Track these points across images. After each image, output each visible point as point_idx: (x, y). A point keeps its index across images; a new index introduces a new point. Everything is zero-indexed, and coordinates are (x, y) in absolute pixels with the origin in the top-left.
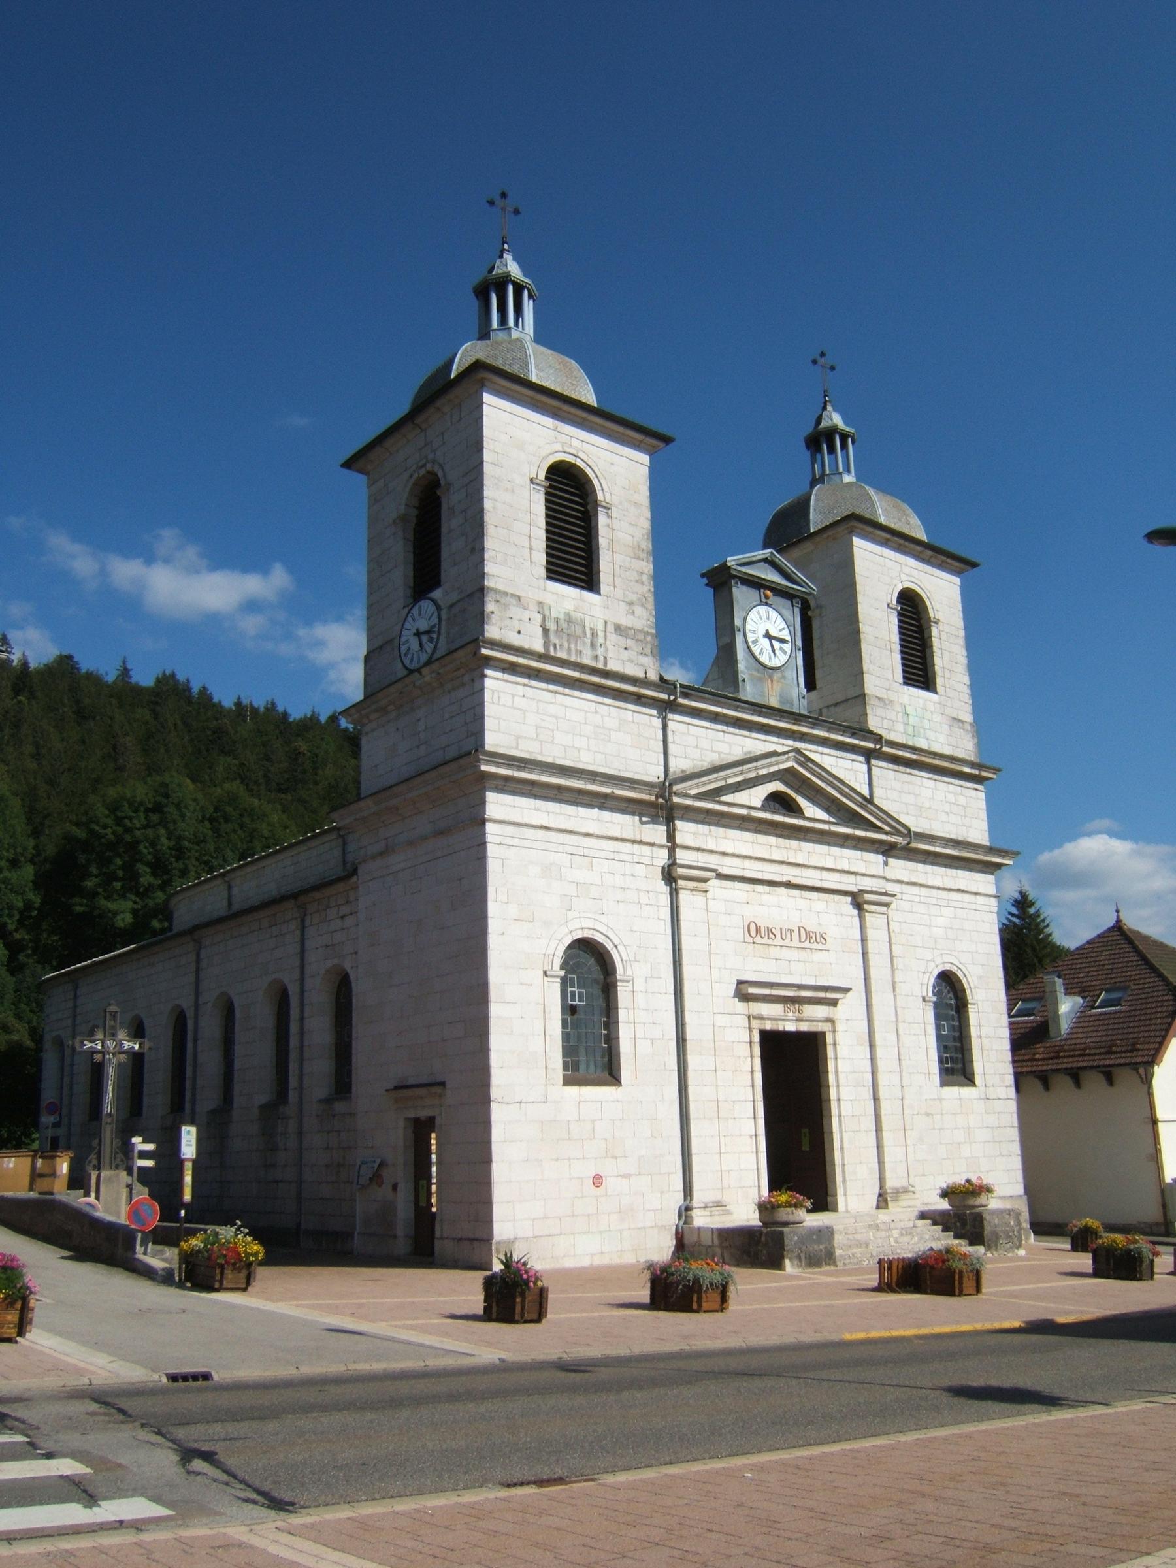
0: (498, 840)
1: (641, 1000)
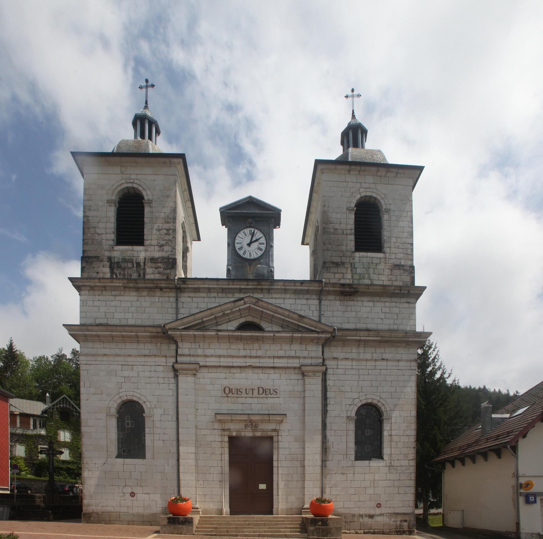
1: (158, 424)
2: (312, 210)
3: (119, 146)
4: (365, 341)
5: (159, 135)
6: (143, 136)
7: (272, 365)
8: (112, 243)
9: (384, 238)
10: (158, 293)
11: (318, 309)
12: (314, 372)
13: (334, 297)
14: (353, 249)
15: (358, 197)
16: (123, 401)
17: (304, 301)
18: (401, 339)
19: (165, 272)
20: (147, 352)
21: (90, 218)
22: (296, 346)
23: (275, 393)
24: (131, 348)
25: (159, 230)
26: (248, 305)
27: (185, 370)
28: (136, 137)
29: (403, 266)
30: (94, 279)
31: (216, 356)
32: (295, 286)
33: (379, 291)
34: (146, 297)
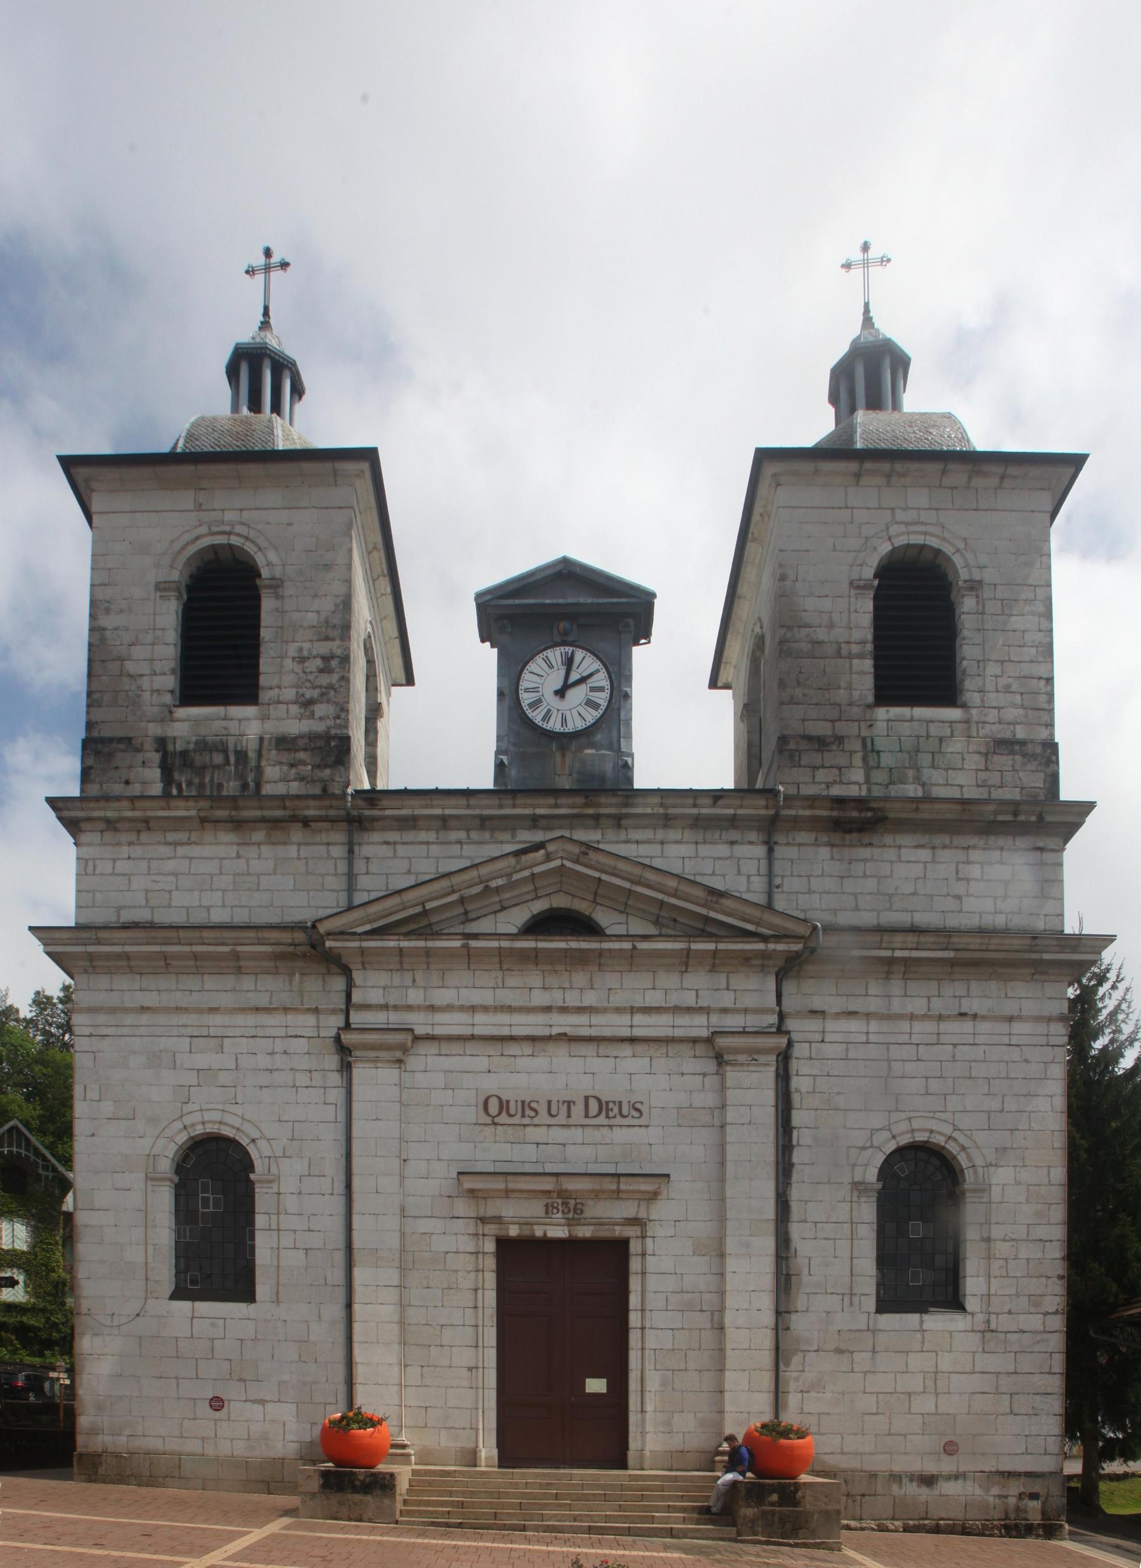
0: (87, 1031)
2: (743, 589)
3: (190, 436)
4: (906, 961)
5: (300, 398)
6: (255, 405)
7: (625, 1032)
8: (168, 699)
9: (965, 663)
10: (297, 834)
11: (764, 870)
12: (752, 1051)
13: (813, 835)
14: (870, 699)
15: (885, 548)
16: (192, 1138)
17: (723, 850)
18: (1017, 956)
19: (319, 774)
20: (263, 1000)
21: (108, 634)
22: (698, 979)
23: (636, 1114)
24: (218, 989)
25: (302, 660)
26: (558, 863)
27: (373, 1047)
28: (235, 408)
29: (1022, 743)
30: (118, 799)
31: (462, 1008)
32: (695, 806)
33: (948, 816)
34: (263, 848)
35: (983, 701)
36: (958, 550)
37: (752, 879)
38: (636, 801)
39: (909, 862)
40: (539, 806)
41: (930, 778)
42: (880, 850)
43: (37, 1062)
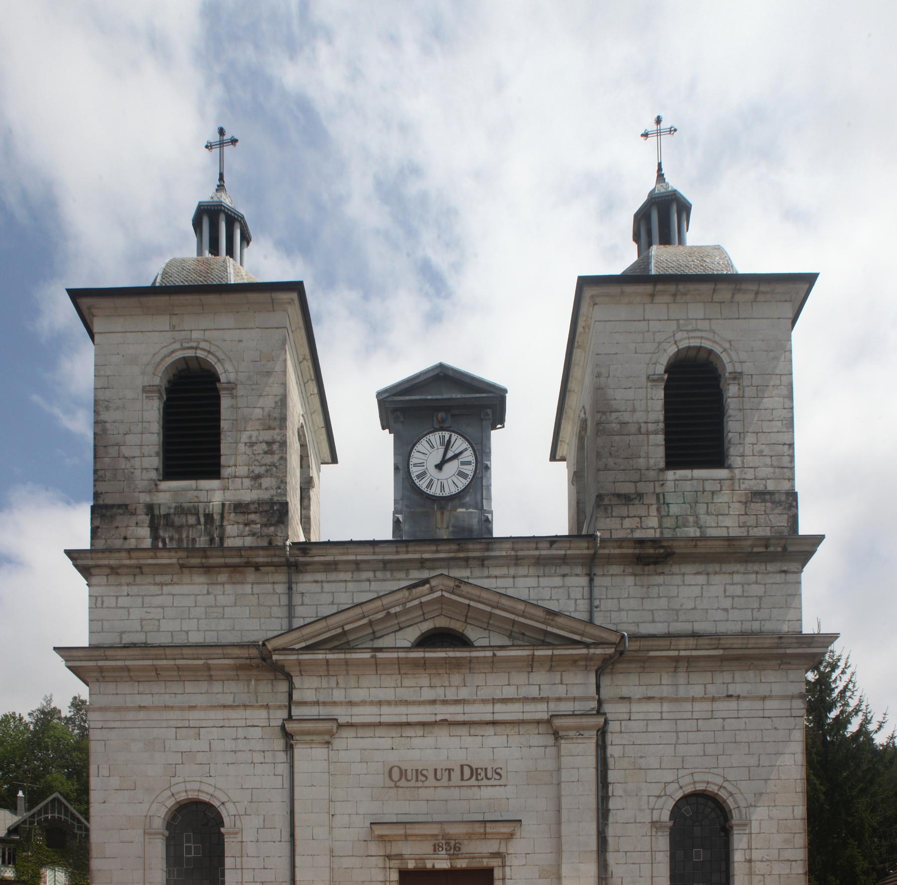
0: (99, 725)
1: (250, 849)
2: (572, 385)
3: (165, 273)
4: (689, 659)
5: (248, 244)
6: (214, 249)
7: (489, 717)
8: (153, 475)
9: (730, 435)
10: (251, 576)
11: (586, 595)
12: (579, 729)
13: (622, 568)
14: (662, 465)
15: (672, 350)
16: (178, 803)
17: (557, 581)
18: (768, 651)
19: (266, 531)
20: (228, 699)
21: (108, 425)
22: (540, 677)
23: (497, 777)
24: (196, 692)
25: (252, 444)
26: (439, 594)
27: (308, 733)
28: (200, 252)
29: (771, 493)
30: (119, 550)
31: (372, 703)
32: (537, 549)
33: (718, 550)
34: (227, 586)
35: (743, 463)
36: (725, 350)
37: (578, 602)
38: (495, 546)
39: (690, 585)
40: (425, 552)
41: (705, 522)
42: (669, 577)
43: (74, 749)
